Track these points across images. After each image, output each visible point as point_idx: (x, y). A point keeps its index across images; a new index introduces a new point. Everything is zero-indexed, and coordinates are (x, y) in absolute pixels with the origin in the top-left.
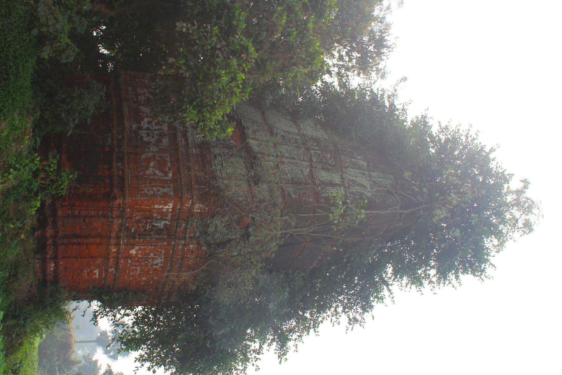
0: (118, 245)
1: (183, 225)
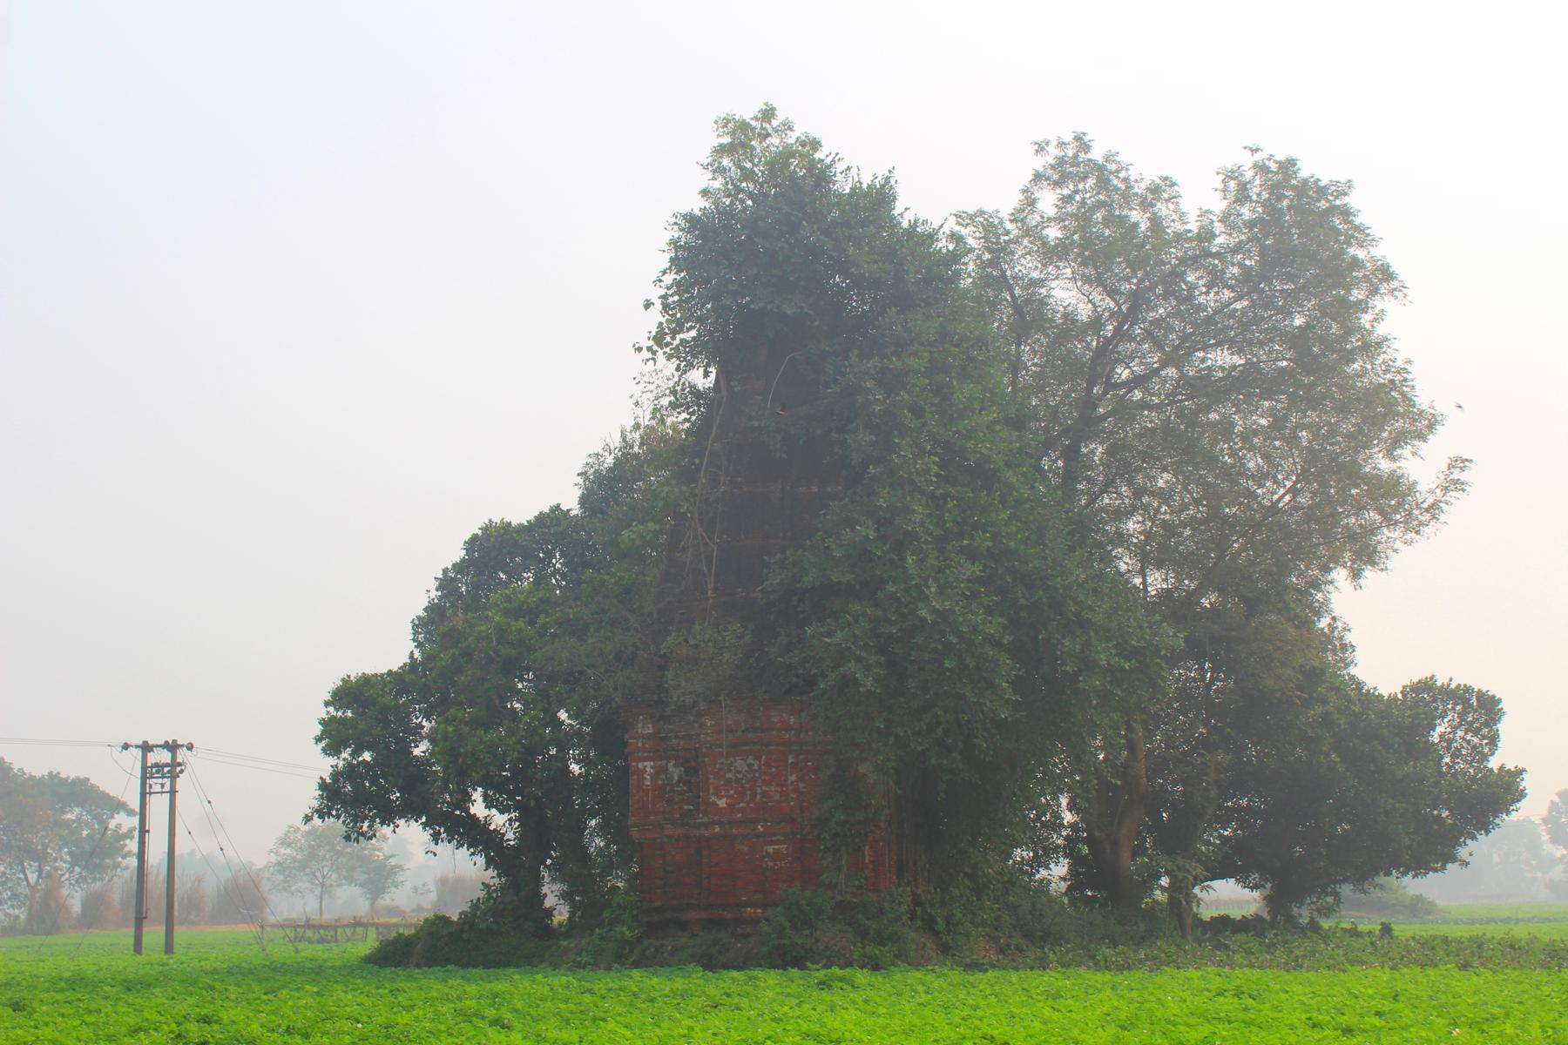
0: (708, 826)
1: (675, 741)
